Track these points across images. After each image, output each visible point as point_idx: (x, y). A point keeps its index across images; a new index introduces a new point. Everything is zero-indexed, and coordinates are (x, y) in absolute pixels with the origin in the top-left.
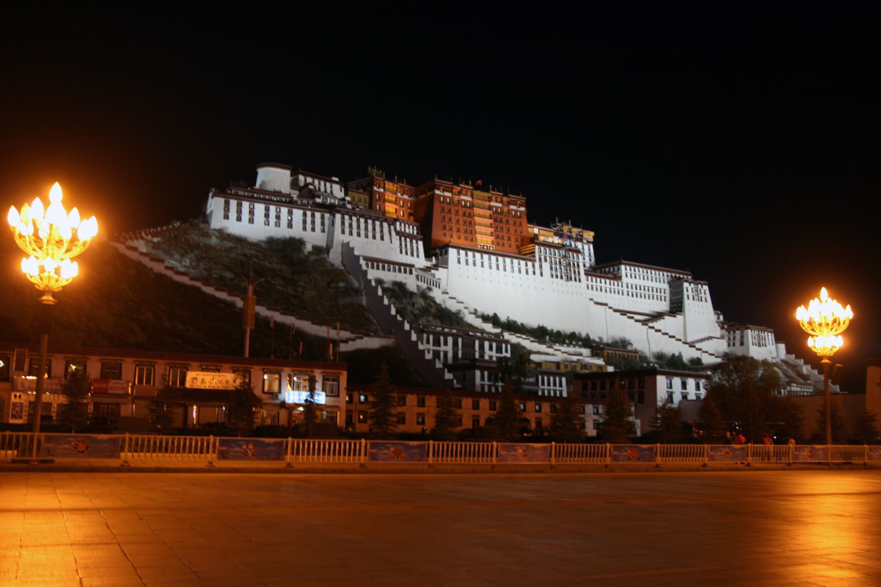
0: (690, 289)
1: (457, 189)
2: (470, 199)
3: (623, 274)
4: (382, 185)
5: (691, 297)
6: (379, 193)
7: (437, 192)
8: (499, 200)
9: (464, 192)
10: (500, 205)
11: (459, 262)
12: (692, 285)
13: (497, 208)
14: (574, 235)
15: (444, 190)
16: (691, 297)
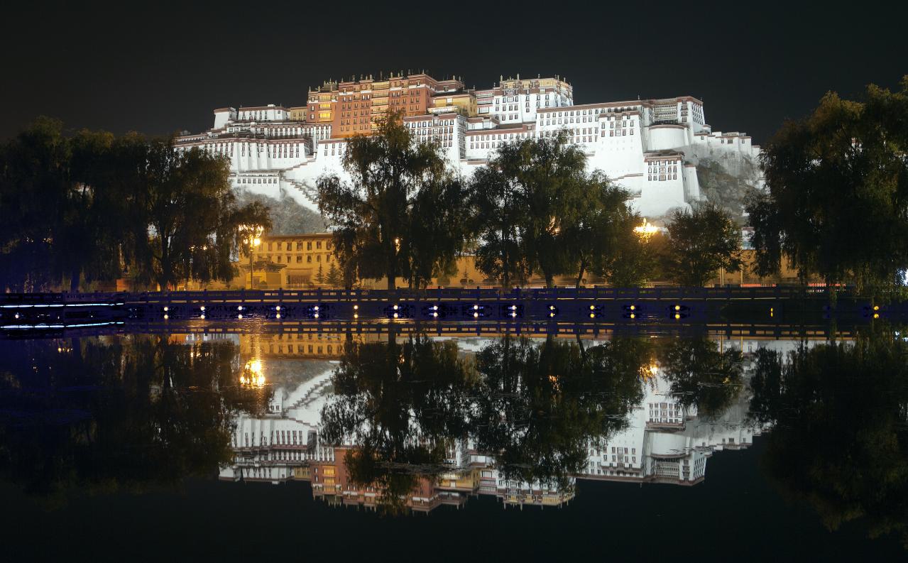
0: (608, 124)
1: (357, 87)
2: (370, 91)
3: (538, 124)
4: (316, 98)
5: (607, 134)
6: (315, 105)
7: (341, 94)
8: (398, 84)
9: (364, 87)
10: (400, 88)
11: (326, 154)
12: (613, 119)
13: (396, 92)
14: (526, 88)
15: (346, 91)
16: (607, 134)
